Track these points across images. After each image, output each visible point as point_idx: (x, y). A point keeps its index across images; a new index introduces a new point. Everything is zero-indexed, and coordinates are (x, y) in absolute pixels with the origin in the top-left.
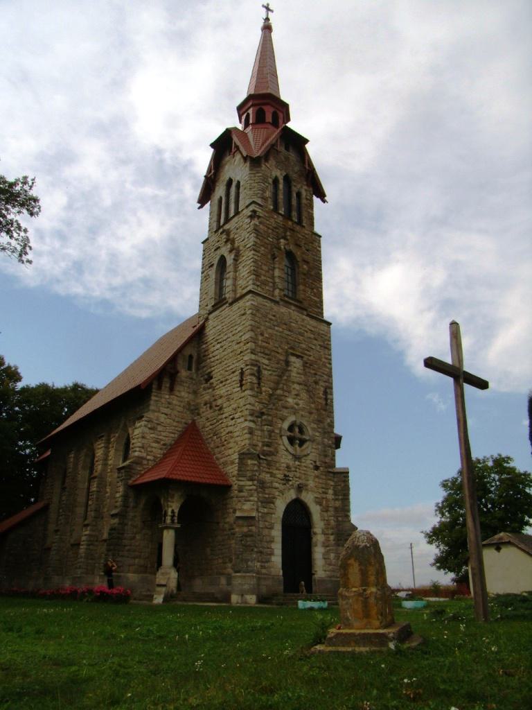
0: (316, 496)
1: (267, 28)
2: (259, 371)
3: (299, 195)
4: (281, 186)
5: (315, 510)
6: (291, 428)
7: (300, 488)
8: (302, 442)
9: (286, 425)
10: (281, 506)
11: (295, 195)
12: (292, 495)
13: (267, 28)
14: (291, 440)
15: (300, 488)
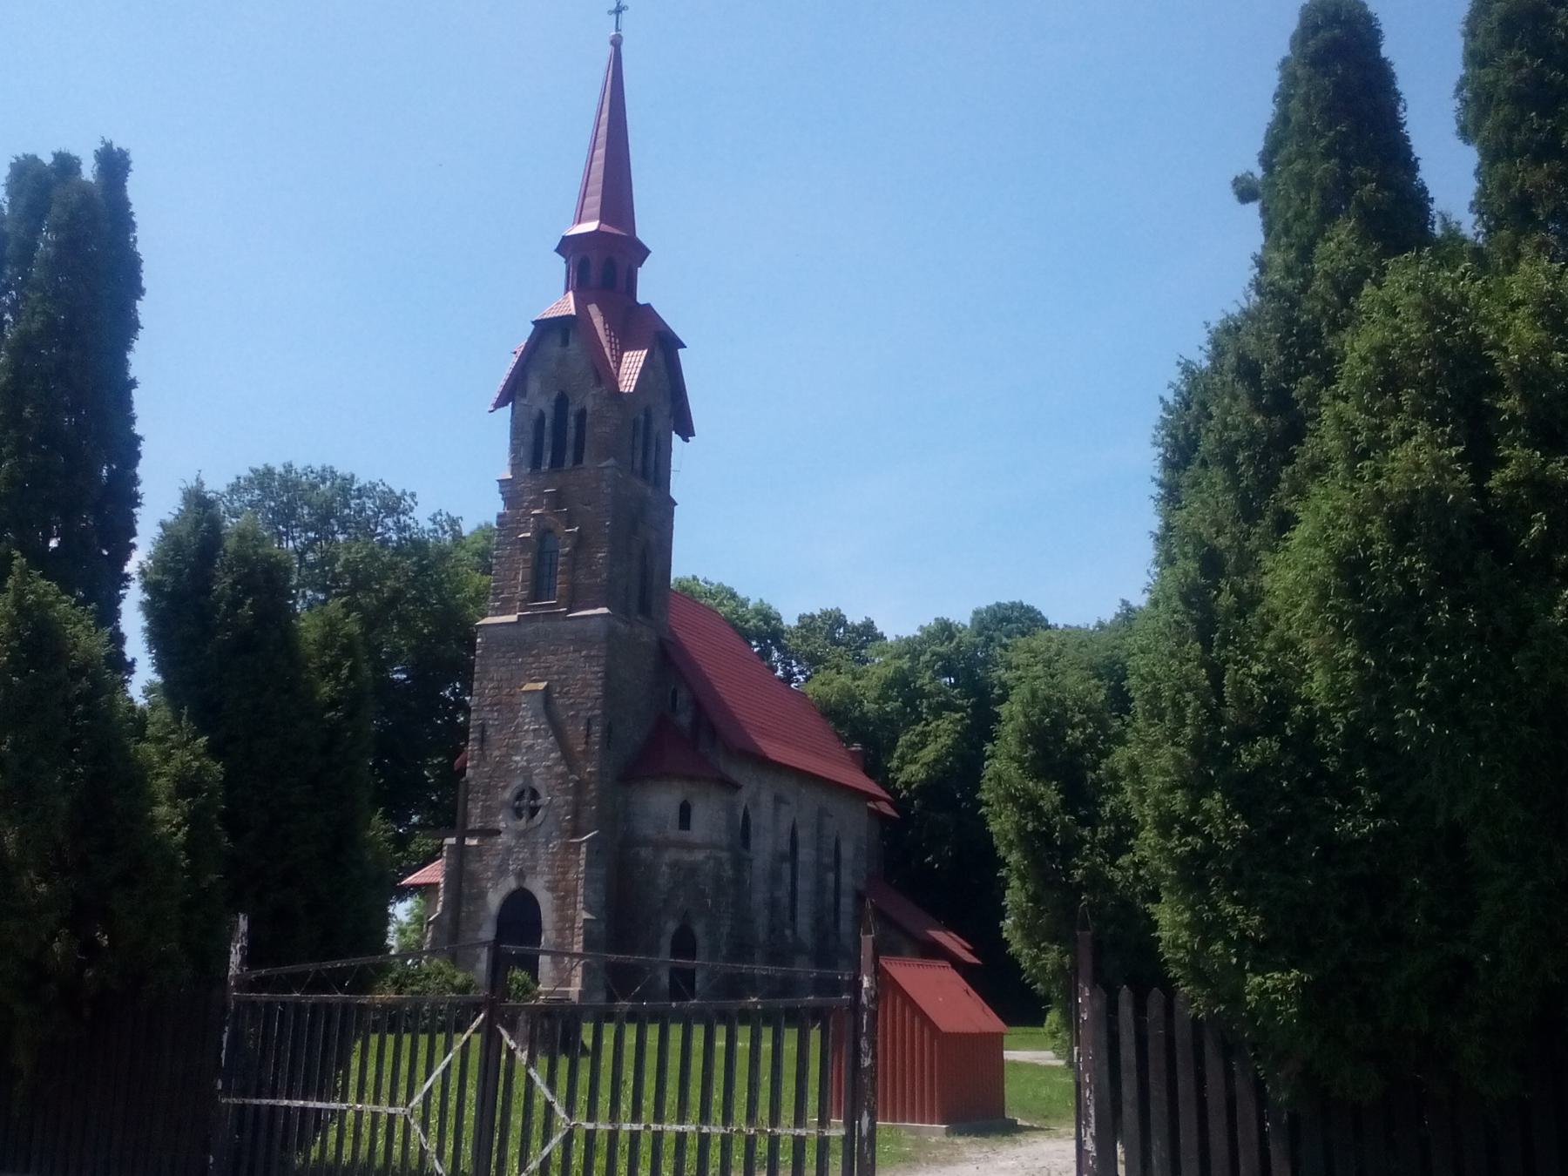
0: (546, 879)
1: (616, 43)
2: (483, 732)
3: (582, 415)
4: (548, 423)
5: (545, 900)
6: (520, 796)
7: (521, 875)
8: (534, 811)
9: (507, 795)
10: (494, 900)
11: (572, 421)
12: (511, 883)
13: (616, 43)
14: (518, 813)
15: (521, 875)
